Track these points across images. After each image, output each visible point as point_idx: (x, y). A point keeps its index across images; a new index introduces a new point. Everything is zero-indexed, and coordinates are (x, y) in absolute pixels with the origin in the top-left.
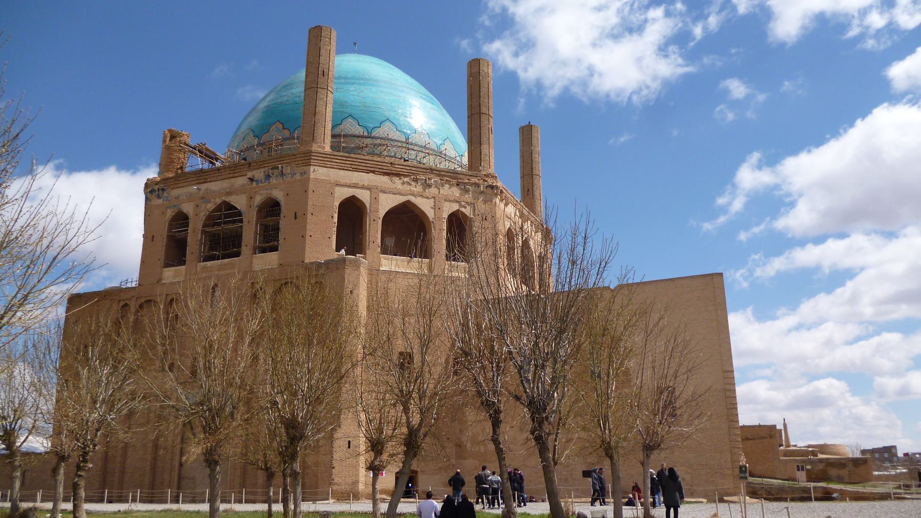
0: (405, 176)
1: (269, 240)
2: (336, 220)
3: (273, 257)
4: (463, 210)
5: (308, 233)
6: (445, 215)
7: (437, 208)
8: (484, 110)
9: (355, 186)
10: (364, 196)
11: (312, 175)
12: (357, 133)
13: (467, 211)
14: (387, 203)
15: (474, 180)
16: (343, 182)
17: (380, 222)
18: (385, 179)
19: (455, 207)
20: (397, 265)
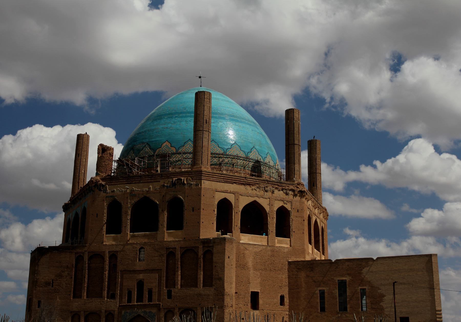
0: (253, 185)
1: (176, 223)
2: (216, 212)
3: (179, 232)
4: (285, 206)
5: (202, 220)
6: (275, 209)
7: (271, 205)
8: (296, 142)
9: (226, 192)
10: (231, 198)
11: (203, 186)
12: (218, 152)
13: (288, 207)
14: (244, 202)
15: (291, 187)
16: (219, 189)
17: (240, 213)
18: (242, 187)
19: (281, 204)
20: (249, 240)
